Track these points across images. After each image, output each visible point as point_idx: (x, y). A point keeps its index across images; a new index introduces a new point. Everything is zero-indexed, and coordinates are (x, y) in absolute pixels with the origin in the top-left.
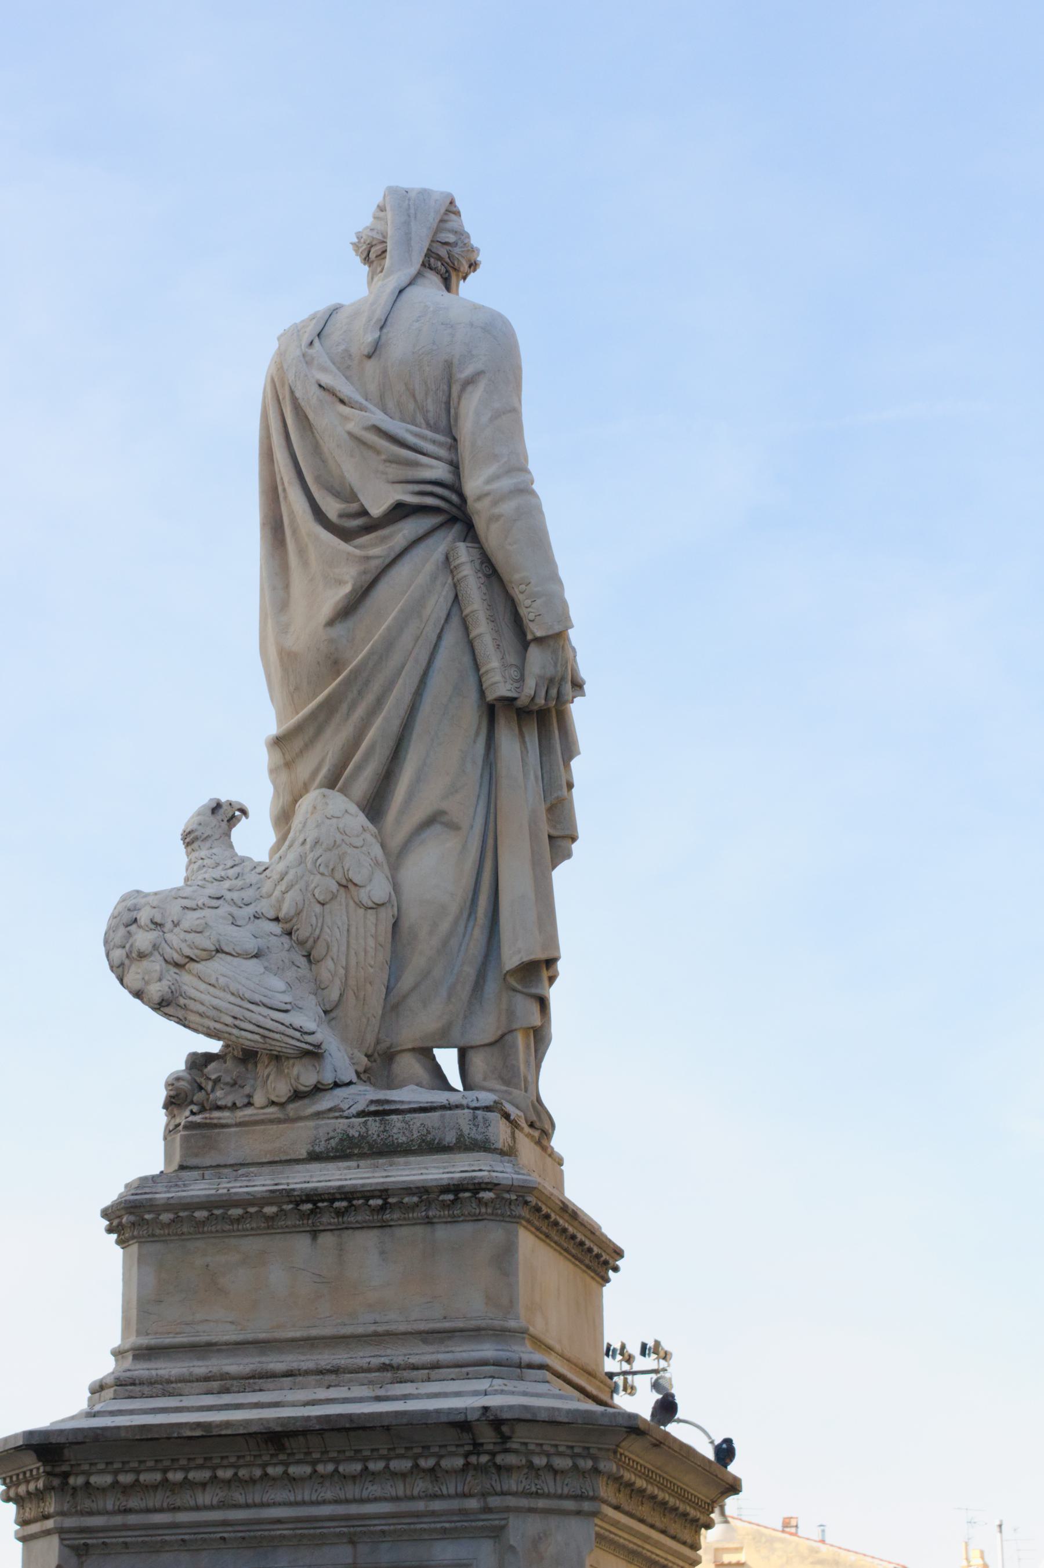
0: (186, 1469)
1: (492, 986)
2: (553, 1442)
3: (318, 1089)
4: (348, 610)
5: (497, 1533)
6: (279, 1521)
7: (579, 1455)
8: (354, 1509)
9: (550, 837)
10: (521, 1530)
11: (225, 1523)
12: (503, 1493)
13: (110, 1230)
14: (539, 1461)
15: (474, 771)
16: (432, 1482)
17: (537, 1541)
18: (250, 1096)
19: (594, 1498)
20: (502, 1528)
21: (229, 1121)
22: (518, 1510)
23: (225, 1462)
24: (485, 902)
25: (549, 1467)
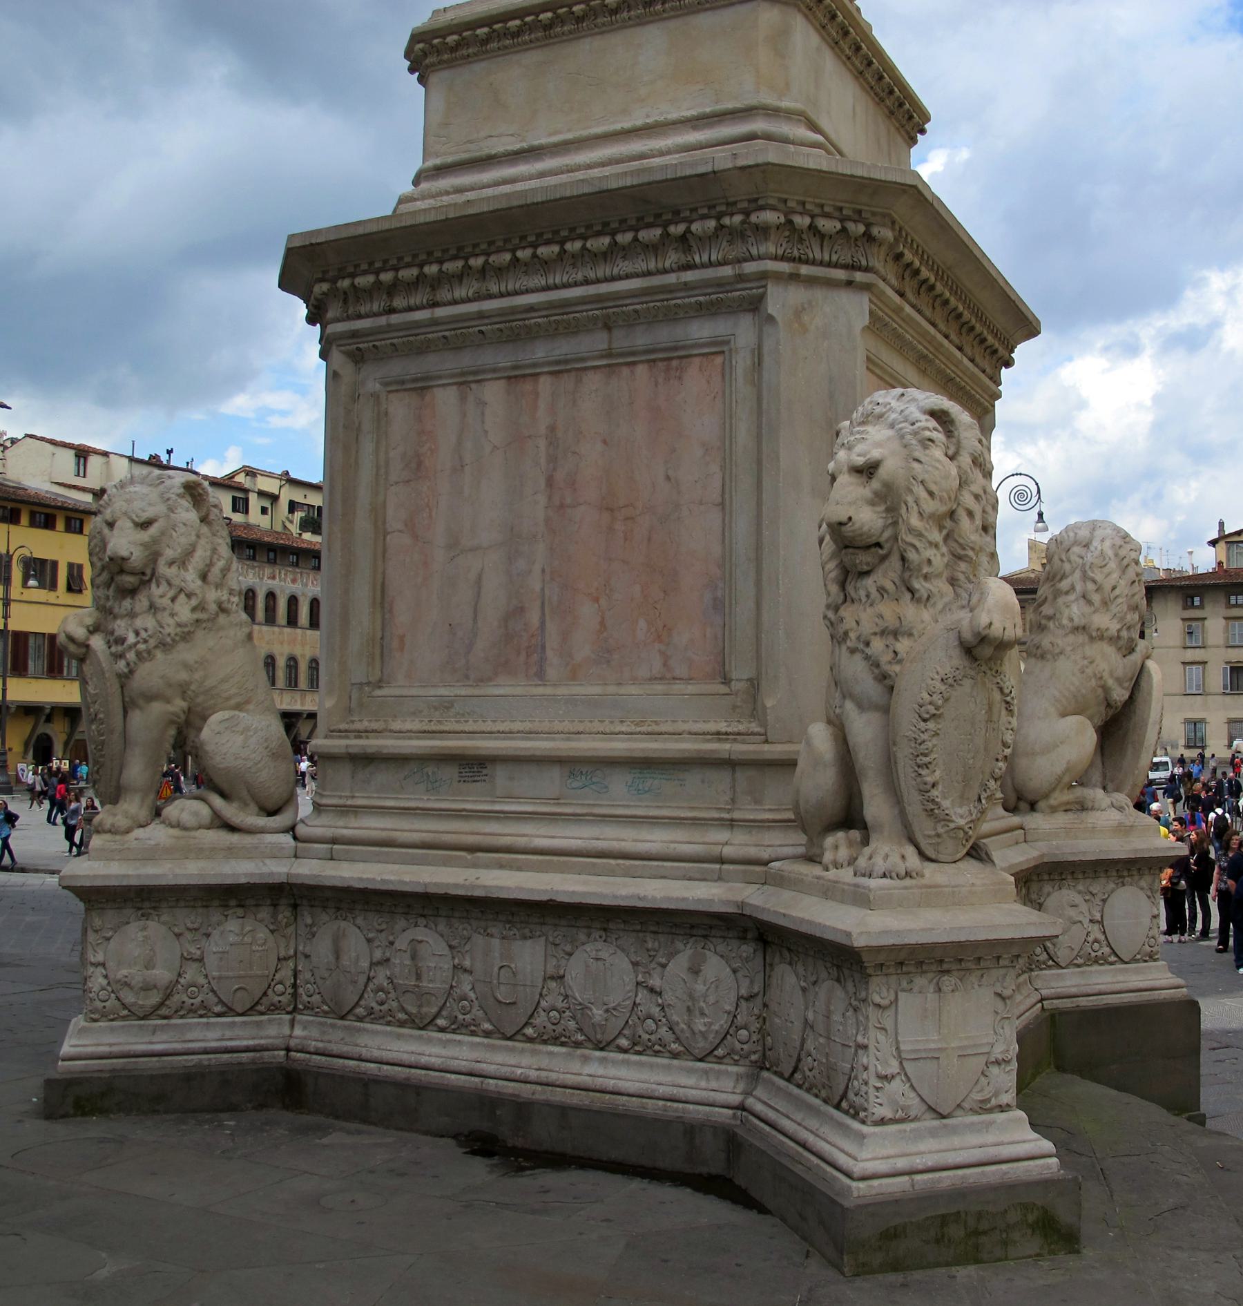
0: (441, 262)
2: (817, 201)
5: (755, 305)
6: (531, 308)
7: (849, 219)
8: (604, 288)
10: (779, 300)
11: (481, 315)
12: (760, 258)
13: (412, 70)
14: (802, 221)
16: (684, 253)
17: (798, 313)
19: (867, 269)
20: (761, 298)
22: (778, 277)
23: (477, 251)
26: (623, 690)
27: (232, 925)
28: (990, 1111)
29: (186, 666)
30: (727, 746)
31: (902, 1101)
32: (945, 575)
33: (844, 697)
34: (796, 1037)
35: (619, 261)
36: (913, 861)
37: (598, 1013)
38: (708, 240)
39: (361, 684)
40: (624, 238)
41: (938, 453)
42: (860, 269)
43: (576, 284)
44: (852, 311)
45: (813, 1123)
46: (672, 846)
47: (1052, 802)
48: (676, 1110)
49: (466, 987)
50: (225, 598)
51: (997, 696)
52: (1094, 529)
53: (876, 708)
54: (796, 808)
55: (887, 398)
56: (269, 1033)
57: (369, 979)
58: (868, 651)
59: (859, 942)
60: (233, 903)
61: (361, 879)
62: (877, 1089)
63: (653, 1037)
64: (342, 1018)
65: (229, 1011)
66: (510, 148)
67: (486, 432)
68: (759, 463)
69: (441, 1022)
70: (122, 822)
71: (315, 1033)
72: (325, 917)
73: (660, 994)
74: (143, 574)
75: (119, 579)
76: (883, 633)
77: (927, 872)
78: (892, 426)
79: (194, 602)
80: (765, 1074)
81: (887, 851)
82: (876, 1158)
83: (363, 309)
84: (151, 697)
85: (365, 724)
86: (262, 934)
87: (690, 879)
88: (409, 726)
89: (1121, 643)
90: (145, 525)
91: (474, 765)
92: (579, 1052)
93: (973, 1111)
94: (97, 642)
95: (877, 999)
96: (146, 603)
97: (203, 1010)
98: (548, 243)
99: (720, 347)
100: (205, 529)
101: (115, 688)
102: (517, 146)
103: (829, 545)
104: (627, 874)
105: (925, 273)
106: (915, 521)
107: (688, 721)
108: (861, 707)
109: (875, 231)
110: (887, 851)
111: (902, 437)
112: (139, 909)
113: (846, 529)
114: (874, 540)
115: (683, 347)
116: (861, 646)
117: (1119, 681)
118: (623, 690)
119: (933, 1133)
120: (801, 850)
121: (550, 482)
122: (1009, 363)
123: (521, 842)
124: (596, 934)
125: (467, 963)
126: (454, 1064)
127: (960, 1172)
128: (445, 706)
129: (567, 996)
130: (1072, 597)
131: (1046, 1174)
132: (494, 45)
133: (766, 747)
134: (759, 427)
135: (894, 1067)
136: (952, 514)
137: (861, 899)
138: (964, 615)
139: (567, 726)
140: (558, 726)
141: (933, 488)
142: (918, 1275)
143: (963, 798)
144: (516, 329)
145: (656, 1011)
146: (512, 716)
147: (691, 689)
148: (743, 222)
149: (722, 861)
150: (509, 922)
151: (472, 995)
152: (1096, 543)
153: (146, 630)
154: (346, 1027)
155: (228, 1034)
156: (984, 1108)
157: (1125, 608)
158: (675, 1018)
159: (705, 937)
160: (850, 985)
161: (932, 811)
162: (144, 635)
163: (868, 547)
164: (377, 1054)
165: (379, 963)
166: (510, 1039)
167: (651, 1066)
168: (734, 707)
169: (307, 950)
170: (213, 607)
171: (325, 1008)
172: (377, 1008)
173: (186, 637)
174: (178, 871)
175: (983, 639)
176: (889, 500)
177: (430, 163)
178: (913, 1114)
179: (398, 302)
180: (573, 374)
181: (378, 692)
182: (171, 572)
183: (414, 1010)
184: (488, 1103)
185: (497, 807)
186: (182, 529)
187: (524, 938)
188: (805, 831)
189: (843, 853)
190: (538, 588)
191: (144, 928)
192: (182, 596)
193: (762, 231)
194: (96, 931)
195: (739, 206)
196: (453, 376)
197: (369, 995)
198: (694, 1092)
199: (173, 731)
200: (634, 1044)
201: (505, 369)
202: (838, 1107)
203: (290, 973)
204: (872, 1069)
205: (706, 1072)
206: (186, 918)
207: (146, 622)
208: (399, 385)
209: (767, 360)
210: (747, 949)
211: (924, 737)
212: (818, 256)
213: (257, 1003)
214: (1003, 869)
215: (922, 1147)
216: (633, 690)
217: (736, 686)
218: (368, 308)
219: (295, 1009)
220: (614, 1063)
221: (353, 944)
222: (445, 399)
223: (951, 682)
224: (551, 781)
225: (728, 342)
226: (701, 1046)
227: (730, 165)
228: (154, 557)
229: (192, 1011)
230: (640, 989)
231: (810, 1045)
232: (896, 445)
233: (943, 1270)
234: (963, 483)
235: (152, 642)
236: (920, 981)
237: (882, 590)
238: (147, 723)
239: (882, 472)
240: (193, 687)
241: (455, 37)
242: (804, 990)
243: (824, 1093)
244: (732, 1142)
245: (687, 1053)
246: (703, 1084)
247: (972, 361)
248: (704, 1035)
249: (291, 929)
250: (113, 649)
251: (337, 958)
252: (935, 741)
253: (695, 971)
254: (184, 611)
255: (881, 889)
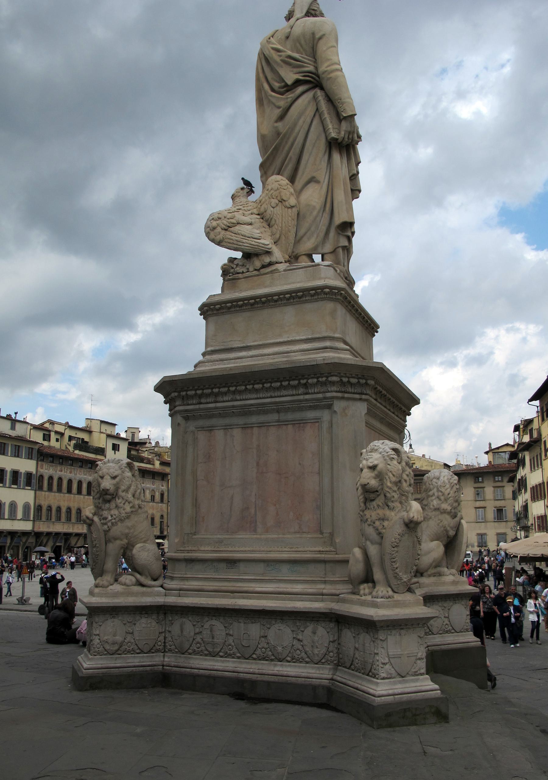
0: (219, 388)
1: (332, 234)
3: (270, 264)
4: (281, 118)
5: (329, 407)
6: (252, 405)
7: (360, 378)
8: (277, 400)
9: (352, 190)
10: (338, 406)
11: (233, 407)
12: (331, 392)
13: (201, 314)
14: (345, 380)
15: (324, 164)
17: (344, 409)
18: (248, 269)
19: (366, 394)
20: (332, 405)
21: (241, 277)
23: (233, 385)
24: (329, 205)
25: (349, 382)
26: (285, 536)
27: (144, 620)
28: (418, 675)
29: (128, 528)
30: (323, 556)
31: (390, 672)
32: (399, 500)
33: (366, 540)
34: (352, 653)
35: (283, 390)
36: (391, 593)
37: (280, 649)
38: (314, 385)
39: (188, 534)
40: (285, 383)
41: (395, 462)
42: (364, 394)
43: (267, 398)
44: (361, 408)
45: (360, 682)
46: (305, 590)
47: (429, 573)
48: (309, 681)
49: (231, 641)
50: (140, 503)
51: (416, 539)
52: (441, 473)
53: (376, 543)
54: (349, 576)
55: (377, 443)
56: (156, 660)
57: (194, 639)
58: (375, 525)
59: (376, 619)
60: (144, 612)
61: (192, 603)
62: (382, 667)
63: (299, 657)
64: (183, 654)
65: (142, 652)
66: (239, 346)
67: (234, 446)
68: (332, 459)
69: (221, 654)
70: (105, 583)
71: (173, 659)
72: (176, 617)
73: (302, 641)
74: (113, 495)
75: (105, 497)
76: (379, 519)
77: (395, 597)
78: (380, 453)
79: (131, 505)
80: (340, 668)
81: (382, 590)
82: (382, 690)
83: (190, 402)
84: (116, 539)
85: (190, 548)
86: (154, 623)
87: (312, 601)
88: (206, 549)
89: (452, 514)
90: (114, 478)
91: (232, 563)
92: (273, 663)
93: (413, 676)
94: (96, 519)
95: (381, 638)
96: (114, 505)
97: (132, 652)
98: (258, 383)
99: (317, 420)
100: (134, 479)
101: (102, 535)
102: (242, 345)
103: (360, 490)
104: (290, 600)
105: (384, 392)
106: (389, 484)
107: (309, 548)
108: (372, 543)
109: (369, 382)
110: (382, 590)
111: (384, 457)
112: (111, 615)
113: (367, 487)
114: (376, 490)
115: (305, 420)
116: (372, 524)
117: (452, 528)
118: (285, 536)
119: (400, 682)
120: (349, 591)
121: (258, 464)
122: (409, 414)
123: (251, 589)
124: (279, 621)
125: (231, 632)
126: (227, 669)
127: (409, 695)
128: (220, 542)
129: (268, 643)
130: (434, 498)
131: (437, 696)
132: (233, 309)
133: (337, 556)
134: (332, 448)
135: (387, 660)
136: (400, 481)
137: (375, 605)
138: (405, 514)
139: (265, 549)
140: (262, 549)
141: (395, 473)
142: (398, 728)
143: (406, 573)
144: (245, 412)
145: (300, 647)
146: (245, 545)
147: (309, 536)
148: (326, 380)
149: (323, 595)
150: (246, 617)
151: (233, 644)
152: (442, 478)
153: (115, 515)
154: (185, 657)
155: (142, 661)
156: (416, 674)
157: (453, 501)
158: (307, 649)
159: (318, 621)
160: (371, 634)
161: (396, 577)
162: (114, 517)
163: (374, 492)
164: (198, 666)
165: (198, 633)
166: (247, 659)
167: (299, 667)
168: (325, 542)
169: (170, 629)
170: (137, 506)
171: (177, 650)
172: (197, 650)
173: (128, 517)
174: (126, 601)
175: (411, 521)
176: (380, 477)
177: (209, 349)
178: (393, 676)
179: (203, 400)
180: (266, 427)
181: (194, 537)
182: (123, 494)
183: (211, 650)
184: (241, 682)
185: (241, 577)
186: (127, 479)
187: (252, 623)
188: (352, 584)
189: (367, 591)
190: (254, 500)
191: (113, 622)
192: (127, 503)
193: (333, 383)
194: (96, 623)
195: (325, 375)
196: (222, 426)
197: (194, 645)
198: (315, 675)
199: (122, 551)
200: (293, 659)
201: (241, 425)
202: (368, 675)
203: (163, 638)
204: (380, 661)
205: (318, 668)
206: (128, 618)
207: (115, 512)
208: (202, 428)
209: (334, 426)
210: (332, 625)
211: (394, 553)
212: (350, 391)
213: (152, 649)
214: (420, 595)
215: (397, 687)
216: (289, 536)
217: (325, 535)
218: (192, 402)
219: (165, 651)
220: (286, 666)
221: (188, 627)
222: (219, 434)
223: (401, 535)
224: (260, 568)
225: (320, 419)
226: (316, 659)
227: (322, 363)
228: (117, 488)
229: (129, 652)
230: (295, 640)
231: (357, 655)
232: (382, 460)
233: (405, 727)
234: (403, 471)
235: (117, 519)
236: (394, 632)
237: (378, 506)
238: (114, 548)
239: (378, 468)
240: (130, 535)
241: (219, 306)
242: (354, 637)
243: (362, 671)
244: (329, 691)
245: (312, 662)
246: (318, 672)
247: (397, 416)
248: (318, 655)
249: (163, 622)
250: (102, 521)
251: (182, 632)
252: (397, 554)
253: (314, 633)
254: (128, 508)
255: (381, 602)
